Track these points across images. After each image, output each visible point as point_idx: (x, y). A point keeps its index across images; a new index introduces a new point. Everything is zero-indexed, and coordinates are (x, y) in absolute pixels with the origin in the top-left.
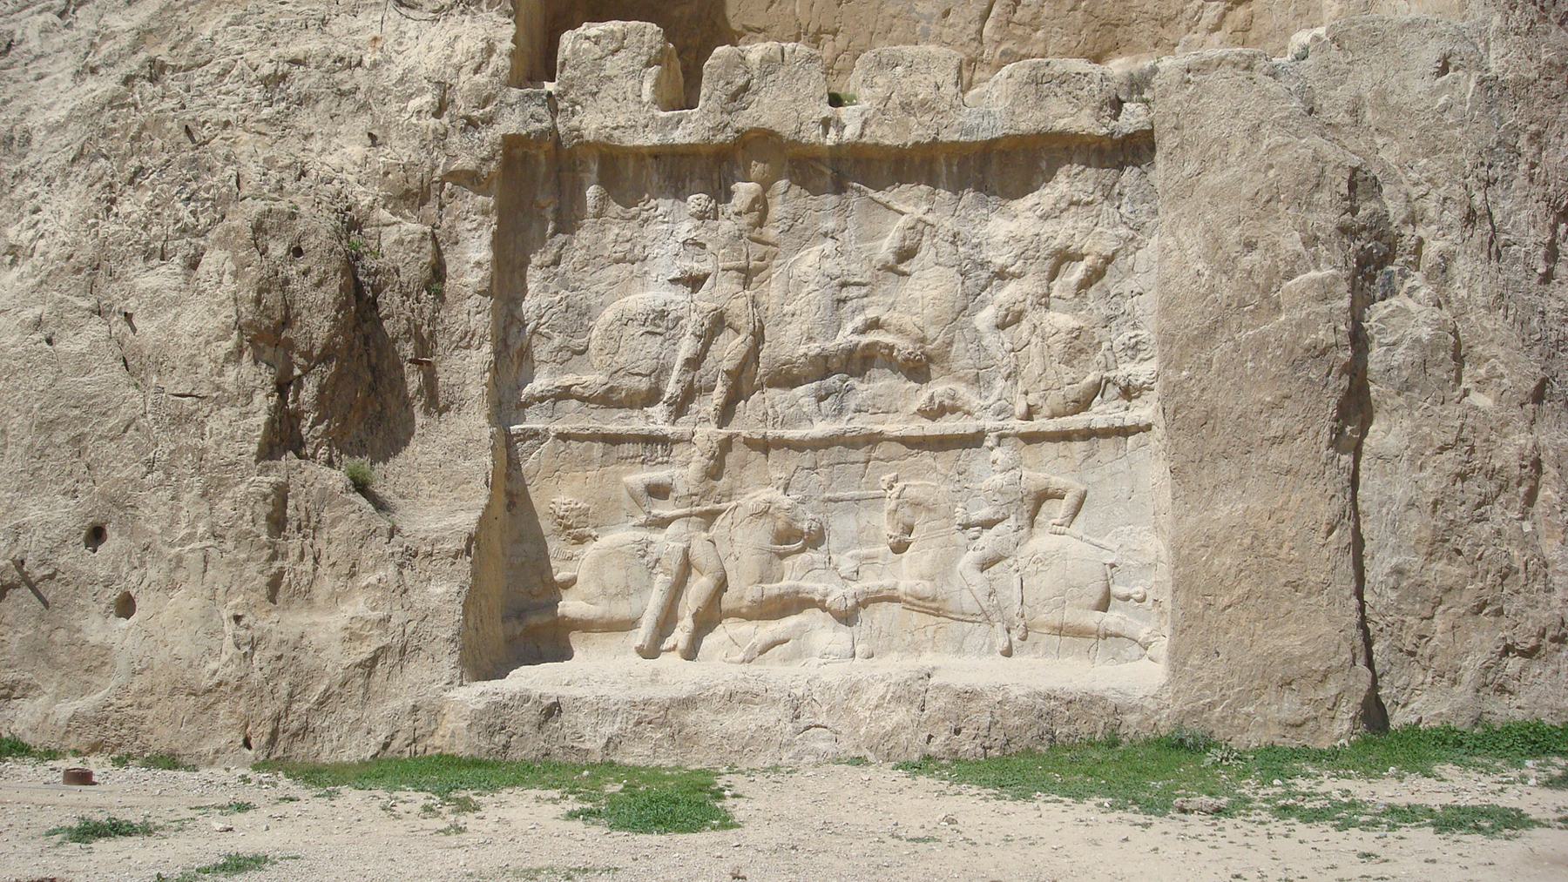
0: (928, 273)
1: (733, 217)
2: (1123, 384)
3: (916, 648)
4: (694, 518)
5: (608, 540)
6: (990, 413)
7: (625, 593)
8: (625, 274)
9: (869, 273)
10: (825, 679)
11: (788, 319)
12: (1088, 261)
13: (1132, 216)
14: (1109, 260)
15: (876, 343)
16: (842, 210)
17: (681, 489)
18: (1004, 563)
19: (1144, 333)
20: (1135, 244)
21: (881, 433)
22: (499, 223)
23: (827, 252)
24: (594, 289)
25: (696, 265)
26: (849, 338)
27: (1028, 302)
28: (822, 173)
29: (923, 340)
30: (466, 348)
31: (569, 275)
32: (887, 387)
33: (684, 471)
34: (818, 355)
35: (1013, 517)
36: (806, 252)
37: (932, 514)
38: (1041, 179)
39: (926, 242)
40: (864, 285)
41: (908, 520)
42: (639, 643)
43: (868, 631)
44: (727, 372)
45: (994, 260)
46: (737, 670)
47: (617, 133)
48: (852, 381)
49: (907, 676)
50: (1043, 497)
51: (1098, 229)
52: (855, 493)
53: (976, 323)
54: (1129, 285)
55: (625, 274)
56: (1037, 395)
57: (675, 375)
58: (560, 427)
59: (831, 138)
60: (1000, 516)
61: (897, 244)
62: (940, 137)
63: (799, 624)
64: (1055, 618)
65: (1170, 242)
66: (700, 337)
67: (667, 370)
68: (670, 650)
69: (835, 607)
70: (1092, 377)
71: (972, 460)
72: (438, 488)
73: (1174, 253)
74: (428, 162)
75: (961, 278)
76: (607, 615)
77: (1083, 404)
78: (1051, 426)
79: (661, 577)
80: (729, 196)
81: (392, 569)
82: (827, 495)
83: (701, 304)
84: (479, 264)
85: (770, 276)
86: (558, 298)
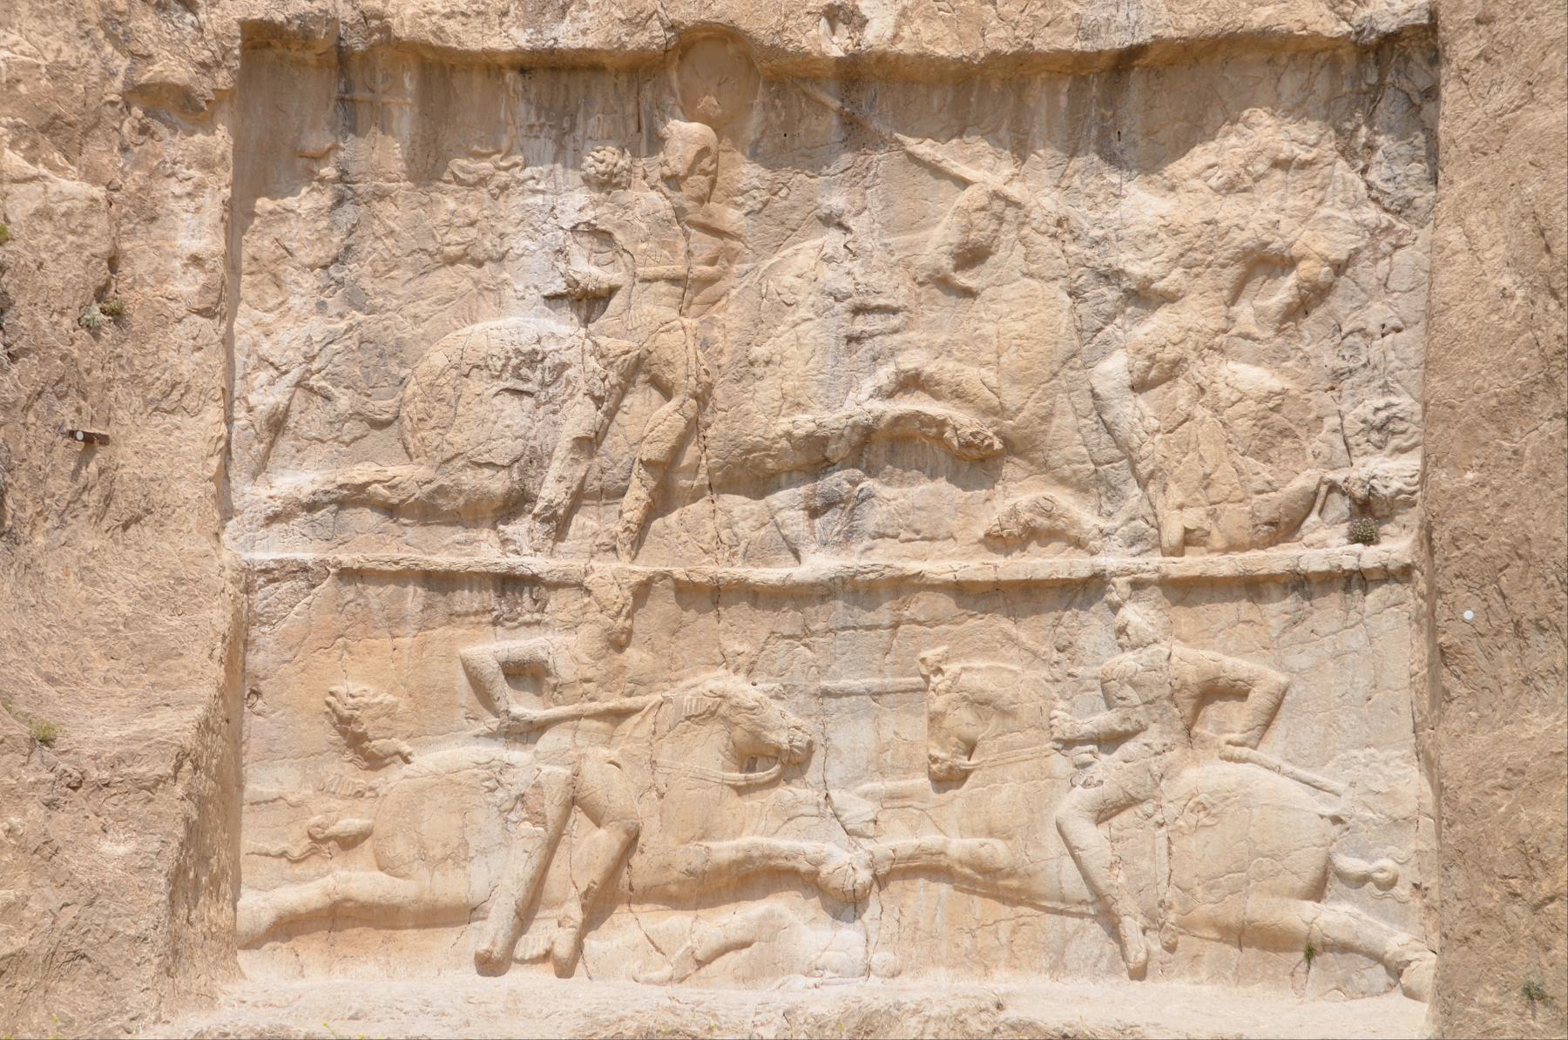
0: (1007, 291)
1: (660, 184)
2: (1360, 493)
3: (981, 962)
4: (584, 723)
5: (430, 760)
6: (1117, 540)
7: (458, 856)
8: (466, 284)
9: (903, 290)
10: (817, 1009)
11: (758, 370)
12: (1305, 269)
13: (1389, 188)
14: (1339, 268)
15: (917, 415)
16: (857, 178)
17: (565, 670)
18: (1138, 810)
19: (1404, 403)
20: (1393, 239)
21: (919, 575)
22: (233, 185)
23: (828, 250)
24: (411, 309)
25: (595, 270)
26: (867, 406)
27: (1190, 345)
28: (825, 106)
29: (999, 411)
30: (172, 412)
31: (366, 283)
32: (933, 494)
33: (571, 639)
34: (809, 436)
35: (1154, 729)
36: (790, 251)
37: (1010, 722)
38: (1220, 118)
39: (1009, 235)
40: (895, 311)
41: (969, 732)
42: (484, 946)
43: (893, 927)
44: (648, 465)
45: (1130, 268)
46: (660, 995)
47: (452, 26)
48: (868, 483)
49: (957, 1005)
50: (1215, 691)
51: (1324, 211)
52: (874, 682)
53: (1095, 382)
54: (1377, 313)
55: (466, 284)
56: (1201, 512)
57: (555, 468)
58: (347, 558)
59: (836, 46)
60: (1128, 727)
61: (955, 238)
62: (1038, 44)
63: (767, 917)
64: (1232, 912)
65: (1454, 236)
66: (598, 401)
67: (541, 459)
68: (534, 961)
69: (836, 882)
70: (1305, 480)
71: (1082, 625)
72: (121, 665)
73: (1460, 257)
74: (95, 63)
75: (1069, 301)
76: (427, 896)
77: (1285, 527)
78: (1226, 565)
79: (527, 826)
80: (656, 142)
81: (35, 811)
82: (825, 683)
83: (603, 341)
84: (196, 260)
85: (726, 293)
86: (343, 325)
